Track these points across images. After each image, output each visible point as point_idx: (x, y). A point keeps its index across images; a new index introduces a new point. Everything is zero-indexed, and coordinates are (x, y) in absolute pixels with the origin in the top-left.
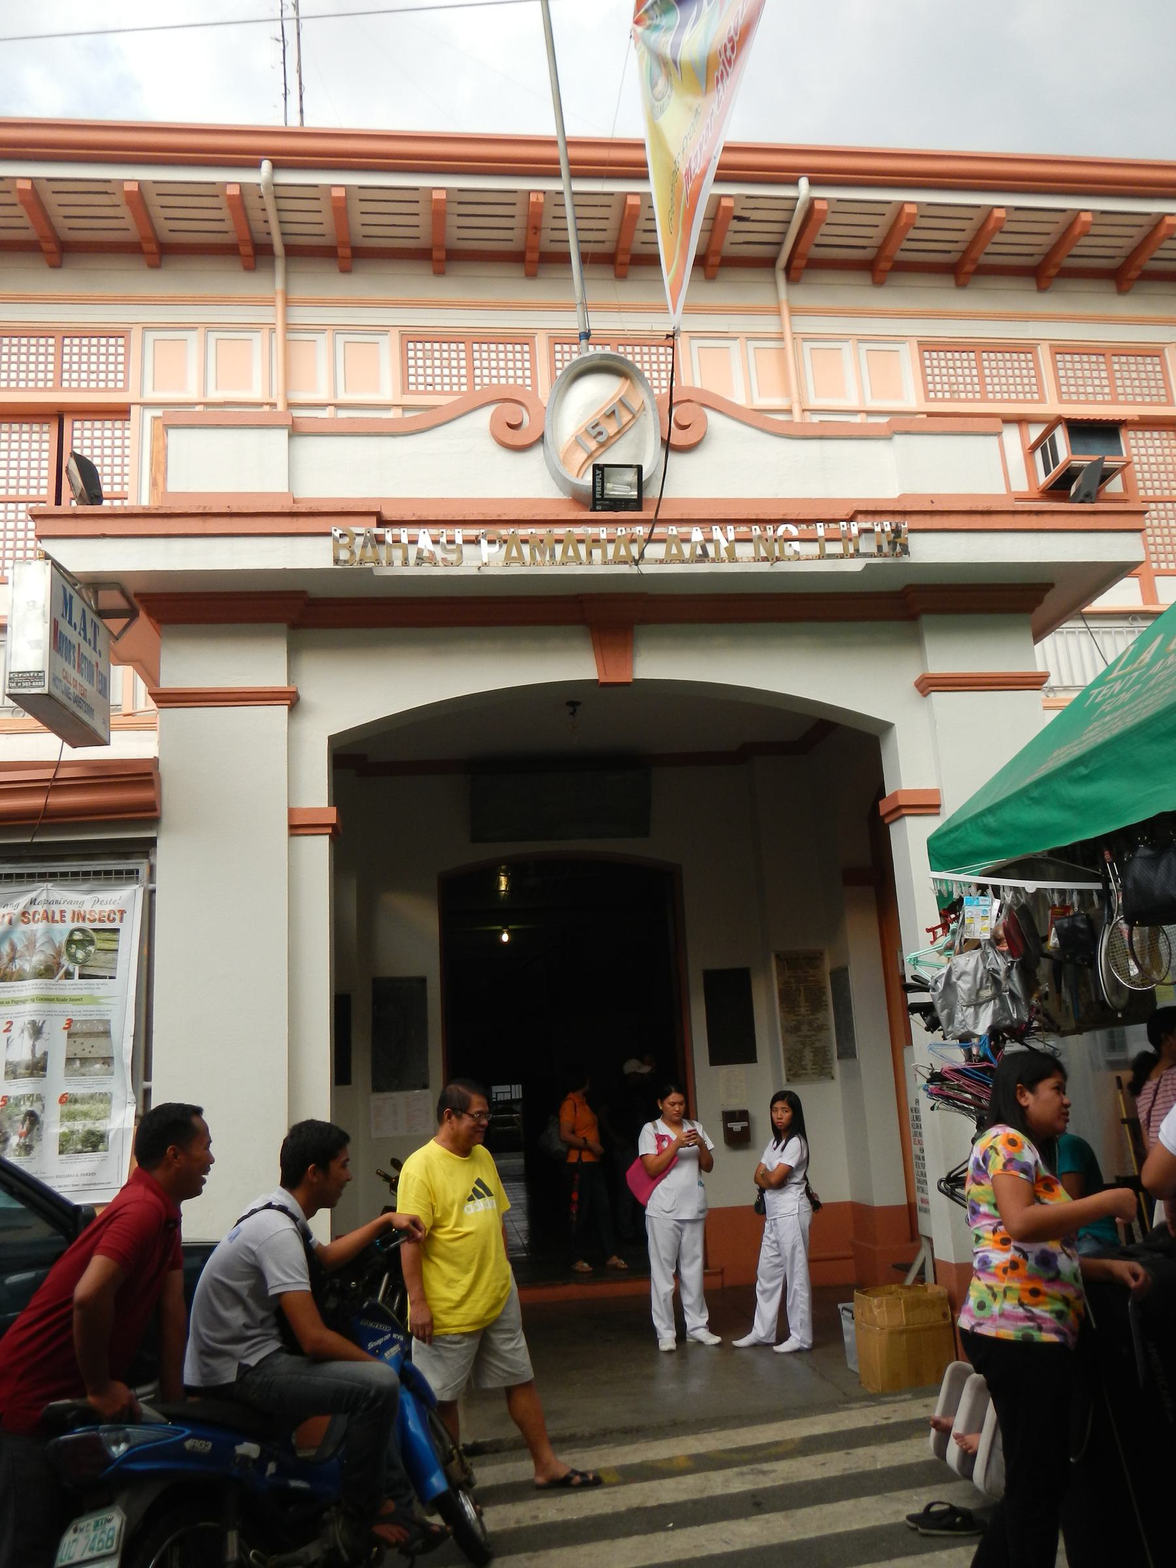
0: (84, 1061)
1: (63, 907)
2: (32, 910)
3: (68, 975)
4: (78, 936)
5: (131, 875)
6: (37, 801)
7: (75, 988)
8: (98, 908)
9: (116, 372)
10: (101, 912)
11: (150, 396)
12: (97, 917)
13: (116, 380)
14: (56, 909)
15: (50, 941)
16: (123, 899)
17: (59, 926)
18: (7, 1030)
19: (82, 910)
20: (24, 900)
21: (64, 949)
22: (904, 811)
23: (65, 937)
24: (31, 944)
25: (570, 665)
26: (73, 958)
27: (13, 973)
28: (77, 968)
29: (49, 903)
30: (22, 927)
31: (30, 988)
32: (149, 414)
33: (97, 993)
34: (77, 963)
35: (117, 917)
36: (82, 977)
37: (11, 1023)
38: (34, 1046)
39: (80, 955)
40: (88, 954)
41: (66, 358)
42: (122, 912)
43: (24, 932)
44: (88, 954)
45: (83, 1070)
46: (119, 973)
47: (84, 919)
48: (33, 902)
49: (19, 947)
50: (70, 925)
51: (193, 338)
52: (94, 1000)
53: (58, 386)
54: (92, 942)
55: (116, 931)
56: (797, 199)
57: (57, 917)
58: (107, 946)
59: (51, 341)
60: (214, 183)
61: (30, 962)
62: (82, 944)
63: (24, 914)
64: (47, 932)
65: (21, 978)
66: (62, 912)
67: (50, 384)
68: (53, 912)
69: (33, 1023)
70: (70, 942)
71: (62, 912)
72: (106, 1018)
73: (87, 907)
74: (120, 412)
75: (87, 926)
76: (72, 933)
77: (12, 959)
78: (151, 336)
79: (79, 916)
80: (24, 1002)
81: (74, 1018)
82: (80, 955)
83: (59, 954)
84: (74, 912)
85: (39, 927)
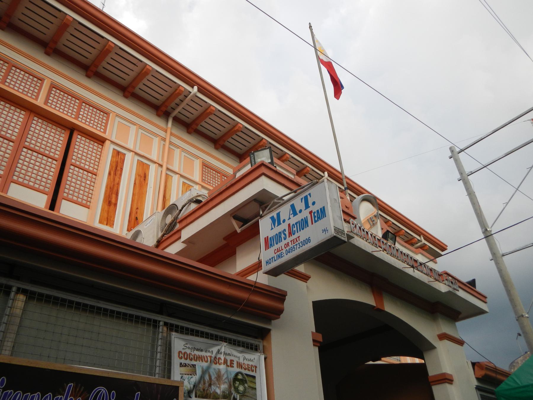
1: (232, 358)
2: (218, 357)
4: (240, 377)
5: (254, 349)
6: (243, 295)
8: (246, 362)
9: (101, 125)
10: (248, 365)
11: (113, 139)
13: (101, 128)
14: (229, 358)
16: (256, 359)
17: (230, 369)
19: (240, 361)
20: (215, 350)
21: (232, 384)
22: (447, 381)
23: (233, 375)
24: (219, 376)
25: (366, 298)
27: (211, 394)
28: (238, 396)
29: (225, 354)
30: (214, 366)
32: (113, 147)
39: (241, 388)
41: (82, 110)
42: (256, 367)
43: (214, 369)
44: (245, 388)
48: (219, 352)
49: (213, 378)
50: (236, 369)
51: (133, 128)
53: (77, 118)
55: (254, 377)
56: (323, 177)
57: (229, 363)
58: (252, 385)
59: (77, 101)
60: (176, 83)
62: (243, 382)
63: (215, 357)
64: (227, 371)
67: (73, 116)
70: (235, 379)
73: (241, 361)
74: (101, 141)
75: (243, 371)
76: (237, 374)
77: (210, 385)
78: (117, 119)
79: (240, 365)
83: (230, 386)
85: (222, 367)
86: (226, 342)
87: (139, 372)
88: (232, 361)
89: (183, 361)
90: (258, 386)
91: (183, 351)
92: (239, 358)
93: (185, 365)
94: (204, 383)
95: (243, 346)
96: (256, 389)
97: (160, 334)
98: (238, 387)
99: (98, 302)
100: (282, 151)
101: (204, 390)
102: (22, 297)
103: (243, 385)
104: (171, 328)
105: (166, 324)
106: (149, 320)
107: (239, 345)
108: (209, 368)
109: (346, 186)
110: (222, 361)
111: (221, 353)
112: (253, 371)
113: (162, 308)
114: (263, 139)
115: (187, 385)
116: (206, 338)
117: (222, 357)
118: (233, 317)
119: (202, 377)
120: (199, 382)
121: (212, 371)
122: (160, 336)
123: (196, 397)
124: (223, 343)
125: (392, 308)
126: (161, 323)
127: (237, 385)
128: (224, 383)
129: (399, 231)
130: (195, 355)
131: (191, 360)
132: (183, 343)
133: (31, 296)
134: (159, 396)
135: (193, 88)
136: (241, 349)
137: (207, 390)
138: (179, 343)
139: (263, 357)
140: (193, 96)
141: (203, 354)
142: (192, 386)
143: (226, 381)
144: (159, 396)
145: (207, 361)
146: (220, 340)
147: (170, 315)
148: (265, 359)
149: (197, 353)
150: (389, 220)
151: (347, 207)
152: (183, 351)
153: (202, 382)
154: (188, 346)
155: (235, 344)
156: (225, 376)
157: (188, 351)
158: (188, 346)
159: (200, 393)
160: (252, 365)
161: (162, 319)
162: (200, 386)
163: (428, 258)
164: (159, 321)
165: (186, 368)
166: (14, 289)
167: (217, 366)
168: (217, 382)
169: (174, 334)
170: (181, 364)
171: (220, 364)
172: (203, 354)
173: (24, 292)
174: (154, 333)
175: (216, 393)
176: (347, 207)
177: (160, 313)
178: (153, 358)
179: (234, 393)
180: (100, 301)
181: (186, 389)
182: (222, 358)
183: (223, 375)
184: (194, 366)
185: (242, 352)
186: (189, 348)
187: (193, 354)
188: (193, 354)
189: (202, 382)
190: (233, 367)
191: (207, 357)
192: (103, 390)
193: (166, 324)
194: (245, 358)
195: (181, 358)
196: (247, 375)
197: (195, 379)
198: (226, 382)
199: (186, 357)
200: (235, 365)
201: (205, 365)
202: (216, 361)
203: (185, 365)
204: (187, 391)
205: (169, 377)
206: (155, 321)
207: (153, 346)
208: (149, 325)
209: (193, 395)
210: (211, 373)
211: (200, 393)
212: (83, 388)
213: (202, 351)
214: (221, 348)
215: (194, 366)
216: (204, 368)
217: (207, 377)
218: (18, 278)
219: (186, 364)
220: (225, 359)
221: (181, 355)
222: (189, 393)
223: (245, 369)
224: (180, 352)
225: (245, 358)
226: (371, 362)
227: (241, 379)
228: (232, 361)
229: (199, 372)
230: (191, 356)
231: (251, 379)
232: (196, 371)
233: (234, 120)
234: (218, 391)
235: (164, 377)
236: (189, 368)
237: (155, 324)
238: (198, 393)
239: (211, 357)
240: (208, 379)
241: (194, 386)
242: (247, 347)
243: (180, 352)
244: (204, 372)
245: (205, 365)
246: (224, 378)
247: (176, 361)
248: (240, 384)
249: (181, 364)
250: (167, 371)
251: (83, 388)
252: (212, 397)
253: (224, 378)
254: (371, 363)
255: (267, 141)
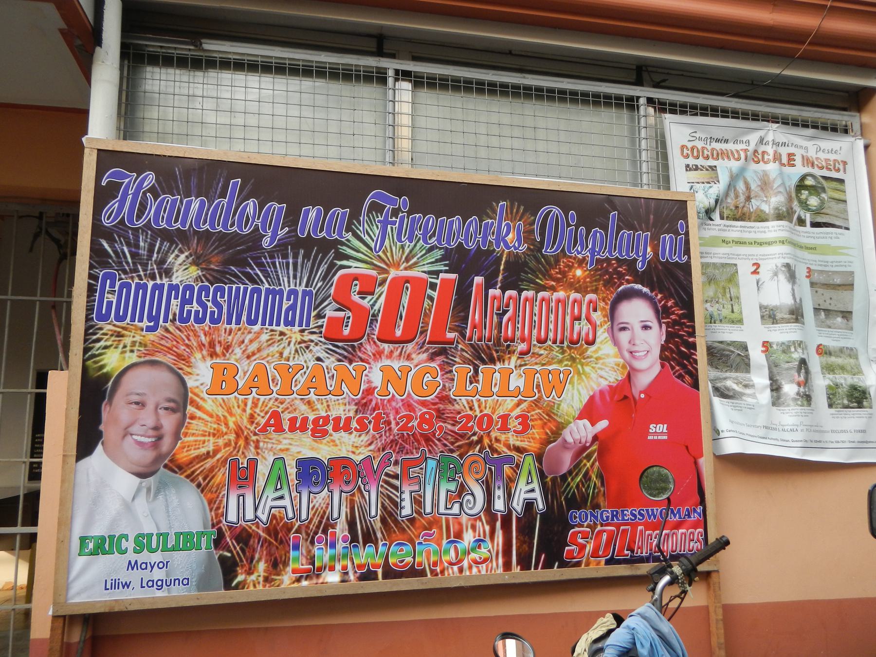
0: (827, 311)
1: (791, 150)
3: (801, 222)
4: (809, 182)
7: (808, 236)
8: (822, 156)
10: (827, 160)
12: (824, 164)
14: (784, 151)
15: (783, 184)
17: (788, 170)
18: (755, 272)
19: (809, 155)
20: (754, 138)
21: (794, 195)
23: (795, 180)
24: (765, 184)
26: (804, 205)
29: (775, 143)
30: (753, 166)
31: (775, 229)
33: (834, 243)
34: (809, 210)
35: (841, 167)
36: (815, 225)
37: (757, 265)
38: (793, 290)
39: (813, 201)
40: (822, 202)
42: (845, 163)
43: (755, 172)
44: (822, 202)
45: (829, 322)
46: (852, 224)
47: (813, 165)
48: (761, 141)
49: (753, 186)
50: (800, 170)
52: (835, 250)
54: (824, 190)
55: (842, 181)
57: (785, 160)
58: (837, 195)
61: (775, 201)
62: (815, 190)
63: (756, 151)
64: (781, 174)
65: (761, 218)
66: (789, 155)
68: (781, 155)
69: (788, 266)
70: (801, 186)
71: (789, 155)
72: (849, 269)
73: (812, 154)
75: (818, 172)
76: (803, 178)
77: (748, 199)
79: (808, 161)
80: (769, 243)
81: (812, 267)
82: (813, 201)
83: (790, 199)
84: (803, 157)
85: (772, 168)
86: (778, 122)
87: (615, 182)
88: (791, 156)
89: (691, 161)
90: (850, 196)
91: (690, 145)
92: (806, 148)
93: (697, 168)
94: (737, 197)
95: (815, 127)
96: (845, 201)
97: (643, 120)
98: (807, 199)
99: (524, 77)
101: (737, 207)
102: (406, 86)
103: (818, 195)
104: (662, 107)
105: (650, 101)
106: (619, 98)
107: (805, 126)
108: (743, 170)
110: (771, 157)
111: (767, 143)
112: (838, 170)
113: (640, 73)
115: (703, 198)
116: (733, 117)
117: (770, 149)
118: (788, 72)
119: (731, 186)
120: (727, 195)
121: (749, 175)
122: (643, 123)
123: (722, 218)
124: (770, 124)
126: (642, 101)
127: (803, 197)
128: (776, 194)
130: (713, 149)
131: (707, 158)
132: (688, 130)
133: (418, 82)
134: (652, 217)
136: (810, 132)
137: (744, 207)
138: (679, 131)
139: (860, 144)
141: (730, 146)
142: (713, 202)
143: (781, 189)
144: (652, 217)
145: (739, 159)
146: (763, 120)
147: (657, 85)
148: (866, 147)
149: (718, 146)
152: (690, 145)
153: (732, 194)
154: (697, 135)
155: (796, 125)
156: (778, 182)
157: (700, 145)
158: (697, 135)
159: (729, 212)
160: (835, 160)
161: (642, 93)
162: (729, 200)
164: (638, 98)
165: (699, 172)
166: (391, 73)
167: (761, 166)
168: (761, 193)
169: (668, 117)
170: (687, 166)
171: (765, 163)
172: (730, 146)
173: (405, 75)
174: (632, 119)
175: (761, 211)
177: (639, 82)
178: (635, 162)
179: (799, 211)
180: (527, 76)
181: (701, 205)
182: (770, 149)
183: (774, 179)
184: (713, 168)
185: (813, 138)
186: (700, 139)
187: (709, 148)
188: (709, 148)
189: (732, 194)
190: (794, 165)
191: (737, 151)
192: (556, 210)
193: (650, 101)
194: (819, 150)
195: (687, 157)
196: (824, 178)
197: (716, 190)
198: (780, 192)
199: (695, 154)
200: (798, 161)
201: (735, 165)
202: (757, 157)
203: (697, 168)
204: (703, 210)
205: (668, 188)
206: (630, 99)
207: (633, 141)
208: (619, 106)
209: (716, 216)
210: (749, 179)
211: (729, 212)
212: (522, 208)
213: (726, 141)
214: (766, 134)
215: (713, 168)
216: (735, 170)
217: (741, 187)
218: (393, 56)
219: (697, 166)
220: (775, 152)
221: (685, 151)
222: (709, 212)
223: (821, 168)
224: (683, 147)
225: (819, 150)
227: (812, 186)
228: (791, 156)
229: (724, 179)
230: (706, 152)
231: (834, 184)
232: (717, 177)
234: (765, 208)
235: (659, 188)
236: (705, 172)
237: (631, 104)
238: (726, 213)
239: (746, 151)
240: (744, 189)
241: (717, 201)
242: (825, 128)
243: (683, 147)
244: (734, 178)
245: (735, 165)
246: (775, 186)
247: (677, 163)
248: (810, 194)
249: (687, 166)
250: (664, 179)
251: (522, 208)
252: (753, 218)
253: (775, 186)
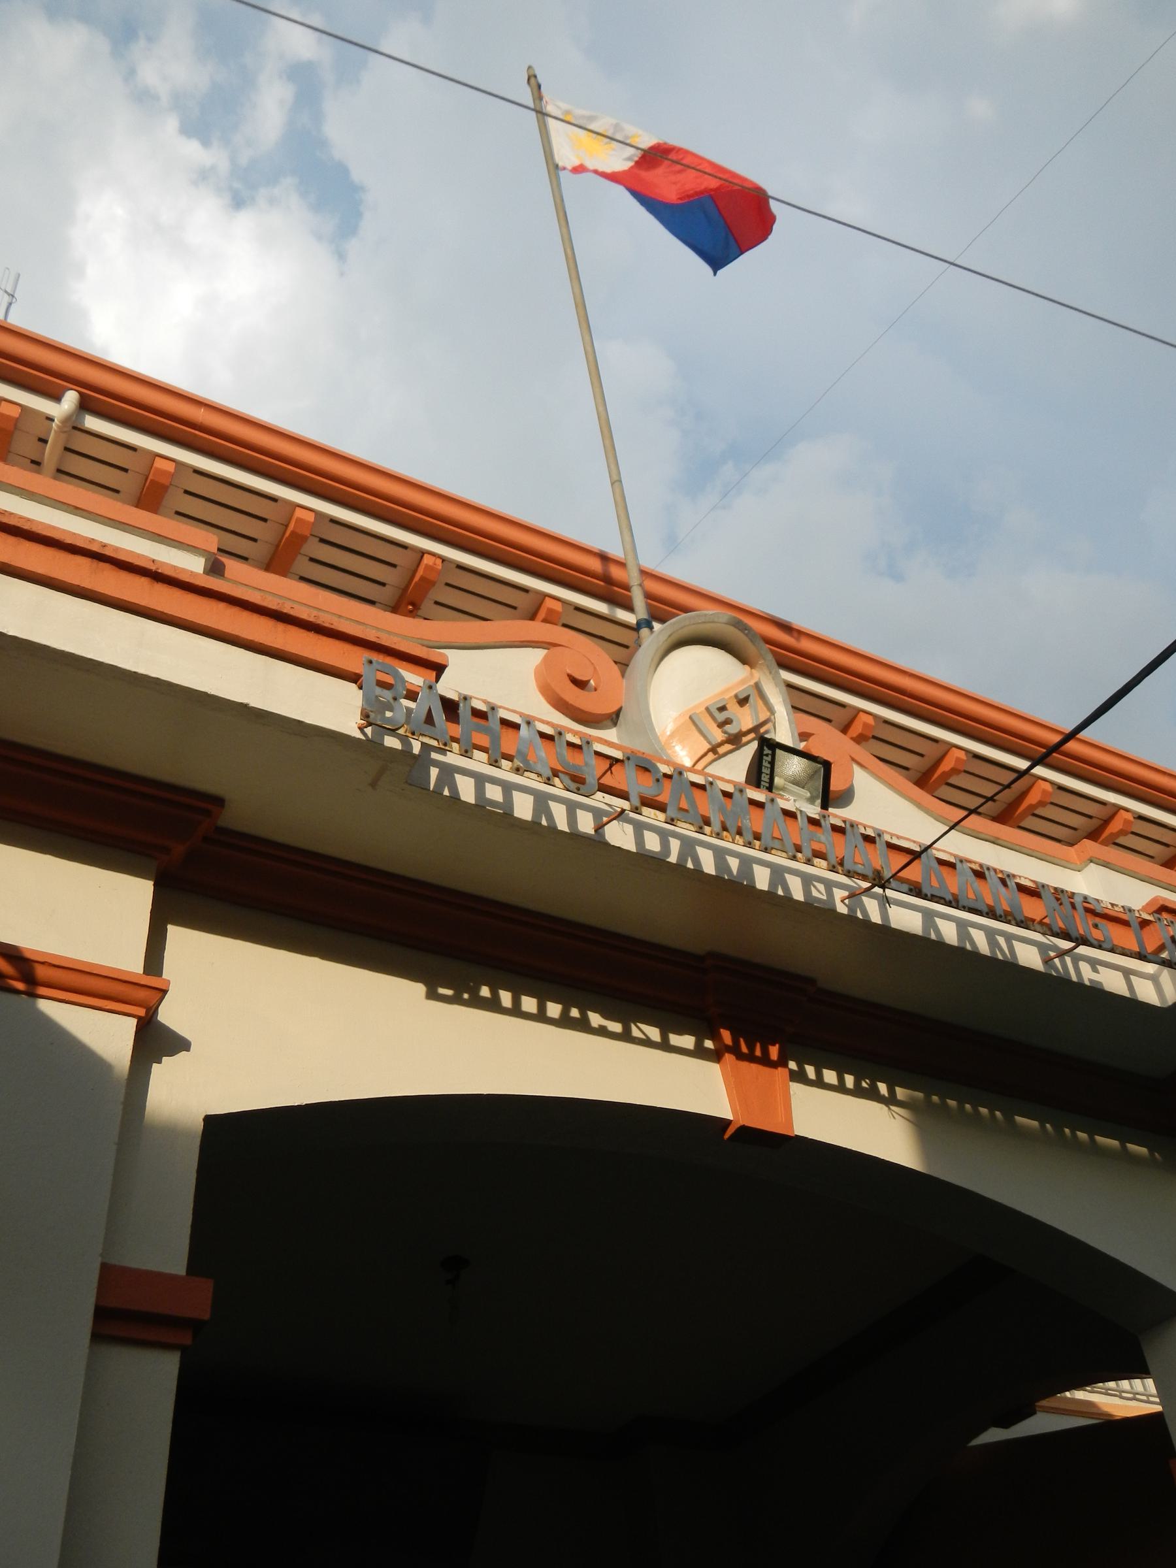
100: (525, 590)
109: (641, 611)
114: (423, 553)
125: (851, 1120)
129: (1106, 822)
135: (57, 398)
140: (61, 430)
150: (1119, 808)
151: (580, 684)
163: (939, 818)
176: (580, 684)
226: (994, 1435)
233: (274, 499)
254: (994, 1435)
255: (444, 560)
